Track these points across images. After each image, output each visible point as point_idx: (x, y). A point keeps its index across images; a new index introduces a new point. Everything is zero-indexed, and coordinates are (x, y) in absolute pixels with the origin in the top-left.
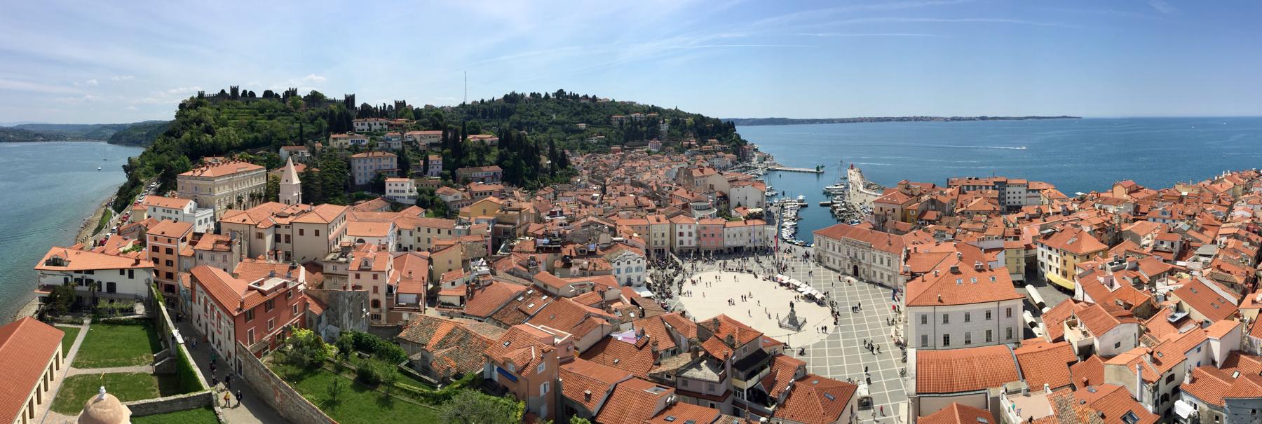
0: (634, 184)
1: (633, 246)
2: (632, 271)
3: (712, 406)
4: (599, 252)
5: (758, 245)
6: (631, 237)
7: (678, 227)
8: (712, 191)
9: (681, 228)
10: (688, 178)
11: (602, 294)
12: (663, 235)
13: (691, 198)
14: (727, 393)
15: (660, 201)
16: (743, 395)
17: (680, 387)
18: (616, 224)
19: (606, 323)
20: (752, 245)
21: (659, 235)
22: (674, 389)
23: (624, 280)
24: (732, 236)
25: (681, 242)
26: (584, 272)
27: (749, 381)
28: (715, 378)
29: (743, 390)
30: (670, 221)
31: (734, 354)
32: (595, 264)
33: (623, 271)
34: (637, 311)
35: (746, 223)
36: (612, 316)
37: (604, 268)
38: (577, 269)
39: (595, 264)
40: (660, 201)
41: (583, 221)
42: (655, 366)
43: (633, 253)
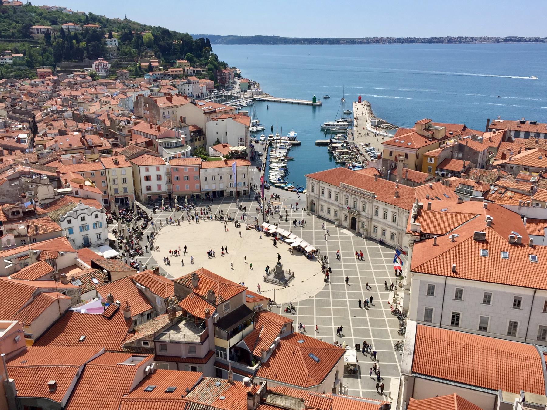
0: (77, 118)
1: (86, 198)
2: (88, 229)
3: (194, 369)
4: (40, 210)
5: (241, 189)
6: (81, 187)
7: (143, 169)
8: (183, 124)
9: (147, 170)
10: (150, 109)
11: (53, 262)
12: (124, 181)
13: (157, 134)
14: (210, 353)
15: (116, 139)
16: (225, 355)
17: (159, 353)
18: (58, 172)
19: (63, 297)
20: (234, 190)
21: (120, 181)
22: (152, 356)
23: (80, 241)
24: (210, 178)
25: (149, 188)
26: (22, 240)
27: (231, 340)
28: (196, 339)
29: (225, 350)
30: (132, 163)
31: (216, 312)
32: (36, 226)
33: (76, 230)
34: (101, 275)
35: (226, 163)
36: (69, 286)
37: (50, 230)
38: (11, 237)
39: (36, 226)
40: (116, 139)
41: (9, 173)
42: (130, 335)
43: (88, 206)
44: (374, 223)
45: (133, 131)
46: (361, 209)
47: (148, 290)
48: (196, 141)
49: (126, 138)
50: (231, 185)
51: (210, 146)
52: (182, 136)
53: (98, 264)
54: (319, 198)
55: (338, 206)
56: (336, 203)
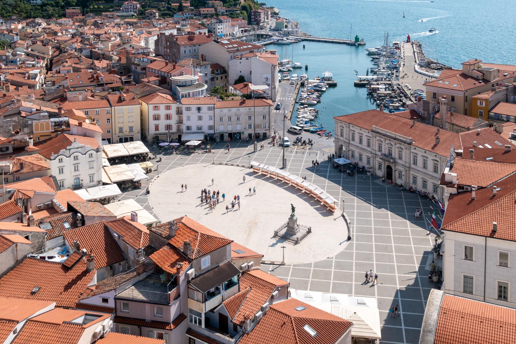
6: (80, 124)
14: (180, 318)
17: (119, 314)
20: (251, 131)
24: (225, 119)
25: (157, 128)
37: (36, 169)
44: (412, 172)
45: (147, 69)
46: (397, 157)
47: (121, 238)
48: (217, 79)
49: (140, 75)
50: (250, 126)
51: (231, 85)
52: (200, 74)
53: (74, 207)
54: (349, 143)
55: (371, 152)
56: (369, 149)
